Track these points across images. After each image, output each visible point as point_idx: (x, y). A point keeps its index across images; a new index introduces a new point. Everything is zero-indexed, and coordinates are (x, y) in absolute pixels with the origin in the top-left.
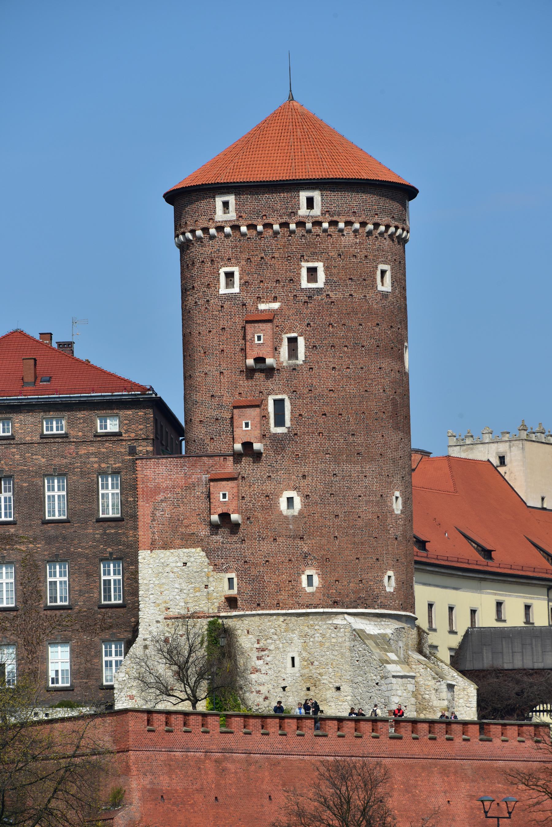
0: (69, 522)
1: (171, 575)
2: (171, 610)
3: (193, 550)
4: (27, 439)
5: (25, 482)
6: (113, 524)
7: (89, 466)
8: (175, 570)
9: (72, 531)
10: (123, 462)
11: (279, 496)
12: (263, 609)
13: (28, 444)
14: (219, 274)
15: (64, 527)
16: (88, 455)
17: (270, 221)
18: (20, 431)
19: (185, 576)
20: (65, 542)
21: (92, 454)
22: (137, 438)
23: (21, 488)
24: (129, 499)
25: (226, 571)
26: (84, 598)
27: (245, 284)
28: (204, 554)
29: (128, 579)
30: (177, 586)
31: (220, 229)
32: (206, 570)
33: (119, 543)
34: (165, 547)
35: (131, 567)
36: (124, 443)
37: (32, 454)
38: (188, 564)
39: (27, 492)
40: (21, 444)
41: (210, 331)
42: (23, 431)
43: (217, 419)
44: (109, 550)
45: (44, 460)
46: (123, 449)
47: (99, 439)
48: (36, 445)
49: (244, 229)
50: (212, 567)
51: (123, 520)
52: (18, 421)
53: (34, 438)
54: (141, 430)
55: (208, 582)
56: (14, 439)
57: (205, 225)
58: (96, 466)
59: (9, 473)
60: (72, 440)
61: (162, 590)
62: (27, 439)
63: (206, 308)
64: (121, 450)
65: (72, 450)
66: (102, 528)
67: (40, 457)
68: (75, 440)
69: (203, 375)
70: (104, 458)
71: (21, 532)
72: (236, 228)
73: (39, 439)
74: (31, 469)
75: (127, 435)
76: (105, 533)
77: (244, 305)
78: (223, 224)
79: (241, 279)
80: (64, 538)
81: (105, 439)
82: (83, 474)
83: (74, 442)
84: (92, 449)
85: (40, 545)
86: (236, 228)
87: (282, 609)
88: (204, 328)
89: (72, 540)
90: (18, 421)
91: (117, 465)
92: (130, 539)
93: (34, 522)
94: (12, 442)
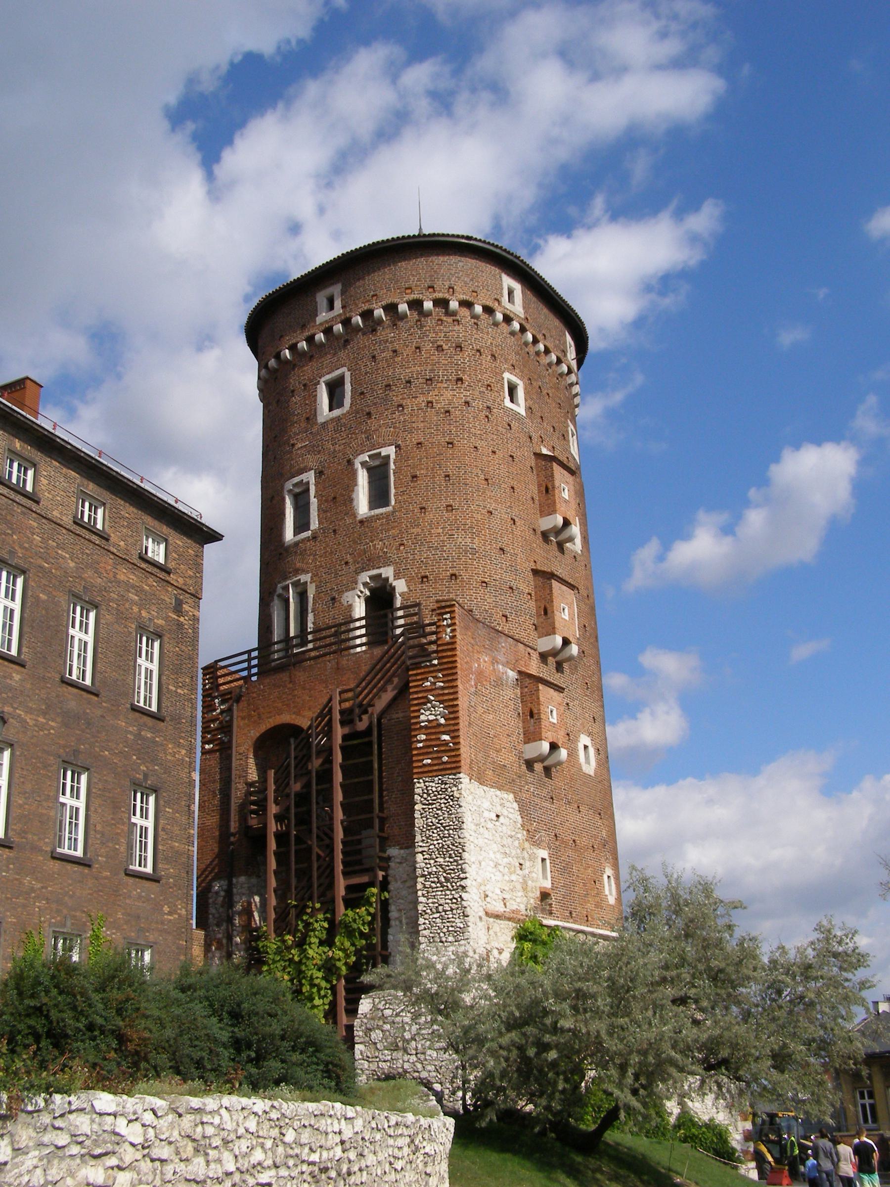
0: (97, 695)
1: (487, 834)
2: (488, 899)
3: (506, 796)
4: (54, 513)
5: (43, 592)
6: (149, 721)
7: (127, 606)
8: (490, 825)
9: (99, 712)
10: (167, 618)
11: (577, 740)
12: (575, 922)
13: (55, 523)
14: (503, 379)
15: (89, 703)
16: (129, 586)
17: (548, 344)
18: (46, 494)
19: (499, 839)
20: (88, 731)
21: (133, 587)
22: (185, 588)
23: (38, 598)
24: (171, 687)
25: (537, 844)
26: (108, 849)
27: (529, 409)
28: (515, 805)
29: (163, 829)
30: (492, 856)
31: (508, 319)
32: (519, 836)
33: (154, 761)
34: (481, 779)
35: (167, 809)
36: (170, 589)
37: (58, 544)
38: (501, 818)
39: (44, 612)
40: (45, 518)
41: (494, 452)
42: (51, 496)
43: (511, 588)
44: (143, 768)
45: (72, 564)
46: (168, 597)
47: (144, 565)
48: (64, 531)
49: (529, 337)
50: (525, 833)
51: (163, 721)
52: (45, 473)
53: (64, 518)
54: (190, 577)
55: (523, 858)
56: (38, 502)
57: (490, 303)
58: (136, 609)
59: (21, 563)
60: (112, 549)
61: (481, 858)
62: (54, 513)
63: (487, 417)
64: (166, 599)
65: (110, 567)
66: (136, 724)
67: (67, 556)
68: (115, 551)
69: (484, 511)
70: (146, 600)
71: (29, 686)
72: (523, 330)
73: (71, 522)
74: (53, 571)
75: (175, 578)
76: (138, 736)
77: (530, 438)
78: (512, 315)
79: (526, 400)
80: (89, 724)
81: (150, 569)
82: (121, 616)
83: (113, 553)
84: (133, 578)
85: (53, 724)
86: (523, 330)
87: (591, 926)
88: (484, 443)
89: (98, 732)
90: (45, 473)
91: (160, 622)
92: (169, 757)
93: (49, 675)
94: (34, 506)
